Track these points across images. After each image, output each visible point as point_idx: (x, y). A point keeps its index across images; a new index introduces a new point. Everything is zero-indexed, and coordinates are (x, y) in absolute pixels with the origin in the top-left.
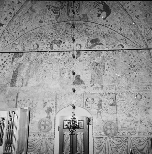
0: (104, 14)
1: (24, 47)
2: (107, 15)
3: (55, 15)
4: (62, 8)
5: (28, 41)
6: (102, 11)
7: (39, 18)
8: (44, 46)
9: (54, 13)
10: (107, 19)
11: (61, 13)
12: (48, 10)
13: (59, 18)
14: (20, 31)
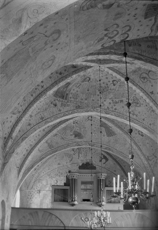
0: (104, 161)
1: (47, 182)
2: (106, 161)
3: (69, 159)
4: (74, 155)
5: (50, 177)
6: (103, 159)
7: (58, 162)
8: (62, 182)
9: (69, 158)
10: (106, 163)
11: (73, 158)
12: (65, 157)
13: (72, 161)
14: (45, 171)
